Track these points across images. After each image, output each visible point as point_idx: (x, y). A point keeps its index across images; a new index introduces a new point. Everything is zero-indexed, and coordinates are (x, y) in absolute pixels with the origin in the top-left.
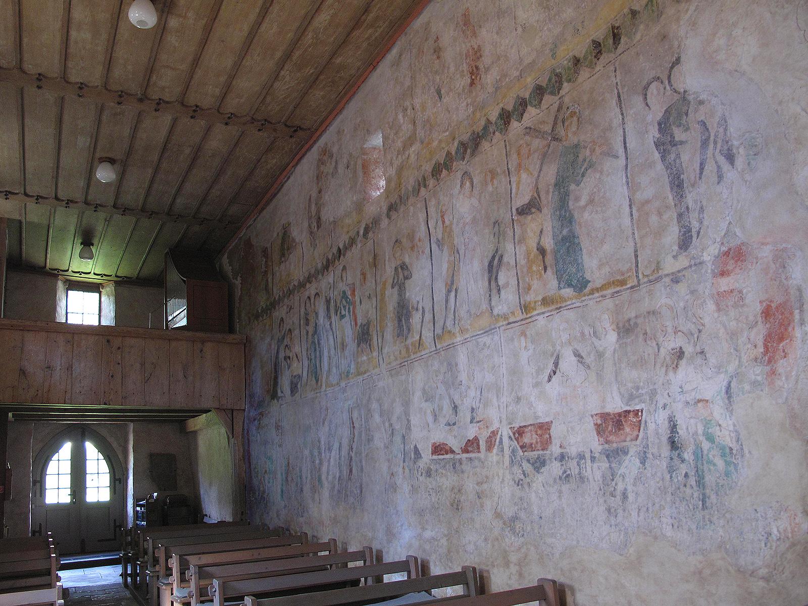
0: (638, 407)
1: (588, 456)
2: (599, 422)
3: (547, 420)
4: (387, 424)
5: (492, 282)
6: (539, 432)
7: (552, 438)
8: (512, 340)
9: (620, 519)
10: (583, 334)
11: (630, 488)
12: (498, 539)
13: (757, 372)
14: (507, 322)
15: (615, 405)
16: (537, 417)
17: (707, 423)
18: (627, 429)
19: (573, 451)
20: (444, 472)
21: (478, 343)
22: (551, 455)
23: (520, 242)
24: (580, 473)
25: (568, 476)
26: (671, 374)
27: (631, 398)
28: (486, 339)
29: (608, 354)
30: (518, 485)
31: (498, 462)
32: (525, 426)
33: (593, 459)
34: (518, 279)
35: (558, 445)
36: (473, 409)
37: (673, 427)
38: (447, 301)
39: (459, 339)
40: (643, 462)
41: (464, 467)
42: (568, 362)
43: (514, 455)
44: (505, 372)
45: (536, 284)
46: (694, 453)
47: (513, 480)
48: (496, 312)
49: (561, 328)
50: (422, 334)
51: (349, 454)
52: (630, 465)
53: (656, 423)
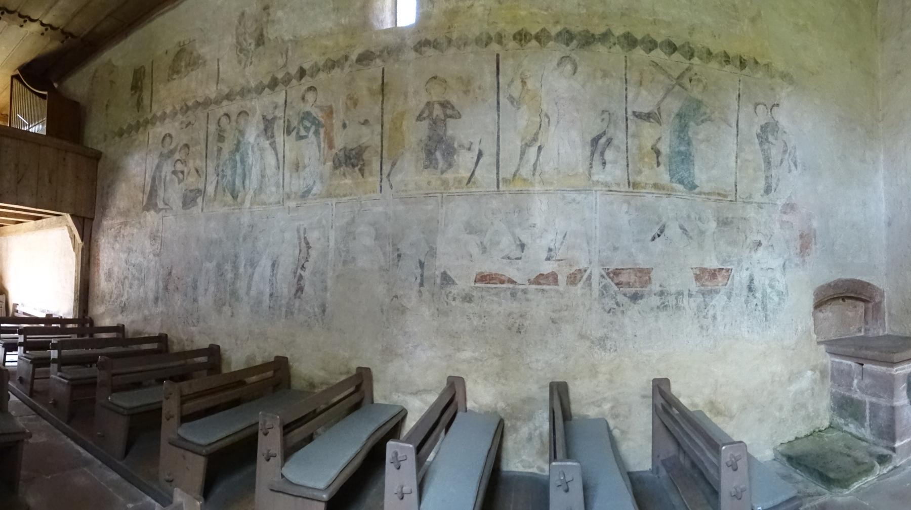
0: (729, 267)
1: (686, 293)
2: (698, 273)
3: (648, 267)
4: (389, 249)
5: (596, 155)
6: (639, 274)
7: (653, 282)
8: (611, 203)
9: (710, 331)
10: (689, 216)
11: (718, 313)
13: (797, 260)
15: (712, 263)
16: (635, 264)
17: (772, 280)
18: (720, 279)
19: (673, 290)
20: (495, 299)
21: (564, 198)
22: (651, 291)
23: (633, 136)
24: (676, 304)
25: (666, 306)
26: (753, 252)
27: (725, 261)
28: (579, 197)
29: (709, 233)
30: (609, 312)
31: (583, 295)
33: (690, 295)
35: (658, 285)
36: (550, 250)
37: (752, 280)
38: (523, 153)
39: (538, 188)
40: (729, 298)
41: (529, 296)
42: (673, 230)
44: (598, 226)
45: (646, 171)
46: (763, 294)
49: (669, 207)
50: (476, 173)
51: (295, 273)
52: (719, 300)
53: (740, 277)
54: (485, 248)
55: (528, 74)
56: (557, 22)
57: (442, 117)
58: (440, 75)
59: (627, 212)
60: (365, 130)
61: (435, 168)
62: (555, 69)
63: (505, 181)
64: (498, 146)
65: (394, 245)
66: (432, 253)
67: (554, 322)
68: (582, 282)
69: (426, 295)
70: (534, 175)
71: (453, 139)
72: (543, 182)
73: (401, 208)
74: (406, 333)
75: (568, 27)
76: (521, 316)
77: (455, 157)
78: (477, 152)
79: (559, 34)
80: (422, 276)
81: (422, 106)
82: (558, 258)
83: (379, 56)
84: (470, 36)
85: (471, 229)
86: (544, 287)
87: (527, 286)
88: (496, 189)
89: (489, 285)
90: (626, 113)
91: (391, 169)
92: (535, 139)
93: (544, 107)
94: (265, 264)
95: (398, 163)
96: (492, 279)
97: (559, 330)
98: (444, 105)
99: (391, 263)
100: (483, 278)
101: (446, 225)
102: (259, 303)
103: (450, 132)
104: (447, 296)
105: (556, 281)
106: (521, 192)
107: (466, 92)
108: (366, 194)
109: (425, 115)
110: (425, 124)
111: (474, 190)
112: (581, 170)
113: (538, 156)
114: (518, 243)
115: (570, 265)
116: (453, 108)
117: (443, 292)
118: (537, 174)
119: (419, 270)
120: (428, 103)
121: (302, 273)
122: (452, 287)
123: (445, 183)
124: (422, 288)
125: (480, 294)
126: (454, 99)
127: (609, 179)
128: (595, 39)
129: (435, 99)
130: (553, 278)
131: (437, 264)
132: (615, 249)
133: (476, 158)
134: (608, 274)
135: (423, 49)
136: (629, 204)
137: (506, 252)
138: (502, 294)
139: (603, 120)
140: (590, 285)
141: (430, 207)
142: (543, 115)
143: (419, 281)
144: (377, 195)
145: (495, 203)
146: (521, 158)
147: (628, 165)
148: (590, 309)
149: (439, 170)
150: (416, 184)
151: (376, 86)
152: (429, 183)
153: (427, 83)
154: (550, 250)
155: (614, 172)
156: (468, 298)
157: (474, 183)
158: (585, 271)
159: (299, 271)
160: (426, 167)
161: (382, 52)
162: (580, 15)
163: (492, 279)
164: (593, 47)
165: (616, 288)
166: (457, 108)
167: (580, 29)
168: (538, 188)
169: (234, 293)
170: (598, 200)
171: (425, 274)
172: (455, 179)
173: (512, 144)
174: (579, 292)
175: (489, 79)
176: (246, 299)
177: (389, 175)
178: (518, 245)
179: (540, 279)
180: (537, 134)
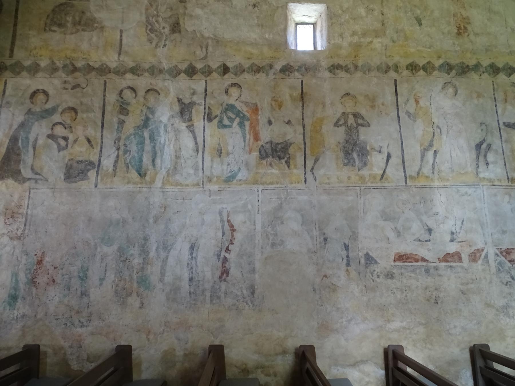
4: (316, 233)
8: (495, 195)
12: (492, 322)
14: (491, 184)
20: (413, 275)
21: (458, 191)
23: (506, 141)
28: (470, 191)
30: (506, 285)
31: (483, 270)
32: (513, 249)
34: (505, 162)
36: (452, 233)
38: (423, 156)
39: (436, 183)
41: (440, 272)
43: (501, 266)
44: (487, 213)
47: (501, 281)
48: (481, 175)
50: (387, 170)
51: (219, 256)
54: (399, 232)
55: (420, 95)
56: (439, 57)
57: (355, 125)
58: (351, 92)
59: (509, 202)
60: (288, 129)
61: (353, 166)
62: (440, 92)
63: (411, 177)
64: (403, 150)
65: (320, 230)
66: (355, 236)
67: (463, 293)
68: (481, 260)
69: (353, 274)
70: (433, 173)
71: (366, 143)
72: (441, 179)
73: (324, 198)
74: (338, 309)
75: (448, 61)
76: (436, 289)
77: (369, 157)
78: (386, 154)
79: (442, 65)
80: (348, 257)
81: (338, 115)
82: (460, 240)
83: (298, 70)
84: (372, 65)
85: (387, 217)
86: (452, 264)
87: (438, 264)
88: (404, 184)
89: (406, 264)
90: (499, 124)
91: (314, 164)
92: (431, 145)
93: (435, 120)
94: (181, 249)
95: (320, 160)
96: (408, 258)
97: (468, 300)
98: (356, 116)
99: (318, 246)
100: (401, 258)
101: (365, 213)
102: (176, 289)
103: (362, 138)
104: (372, 274)
105: (460, 259)
106: (423, 187)
107: (373, 107)
108: (291, 183)
109: (341, 123)
110: (342, 130)
111: (386, 184)
112: (470, 170)
113: (435, 158)
114: (426, 228)
115: (470, 246)
116: (363, 118)
117: (368, 270)
118: (435, 172)
119: (345, 252)
120: (343, 114)
121: (227, 255)
122: (375, 266)
123: (362, 178)
124: (348, 268)
125: (399, 271)
126: (363, 112)
127: (492, 176)
128: (469, 69)
129: (349, 110)
130: (457, 256)
131: (360, 246)
132: (504, 232)
133: (385, 159)
134: (501, 253)
135: (336, 71)
136: (510, 195)
137: (416, 237)
138: (418, 271)
139: (482, 130)
140: (488, 262)
141: (350, 198)
142: (435, 127)
143: (345, 261)
144: (302, 186)
145: (404, 196)
146: (422, 160)
147: (505, 164)
148: (491, 282)
149: (357, 168)
150: (338, 178)
151: (297, 93)
152: (349, 178)
153: (342, 97)
154: (452, 233)
155: (495, 171)
156: (390, 275)
157: (387, 179)
158: (483, 250)
159: (223, 253)
160: (346, 165)
161: (300, 67)
162: (456, 51)
163: (408, 258)
164: (468, 75)
165: (509, 265)
166: (366, 118)
167: (458, 61)
168: (436, 183)
169: (144, 281)
170: (485, 193)
171: (351, 255)
172: (370, 175)
173: (413, 149)
174: (480, 268)
175: (390, 98)
176: (159, 286)
177: (312, 169)
178: (426, 230)
179: (447, 258)
180: (432, 141)
